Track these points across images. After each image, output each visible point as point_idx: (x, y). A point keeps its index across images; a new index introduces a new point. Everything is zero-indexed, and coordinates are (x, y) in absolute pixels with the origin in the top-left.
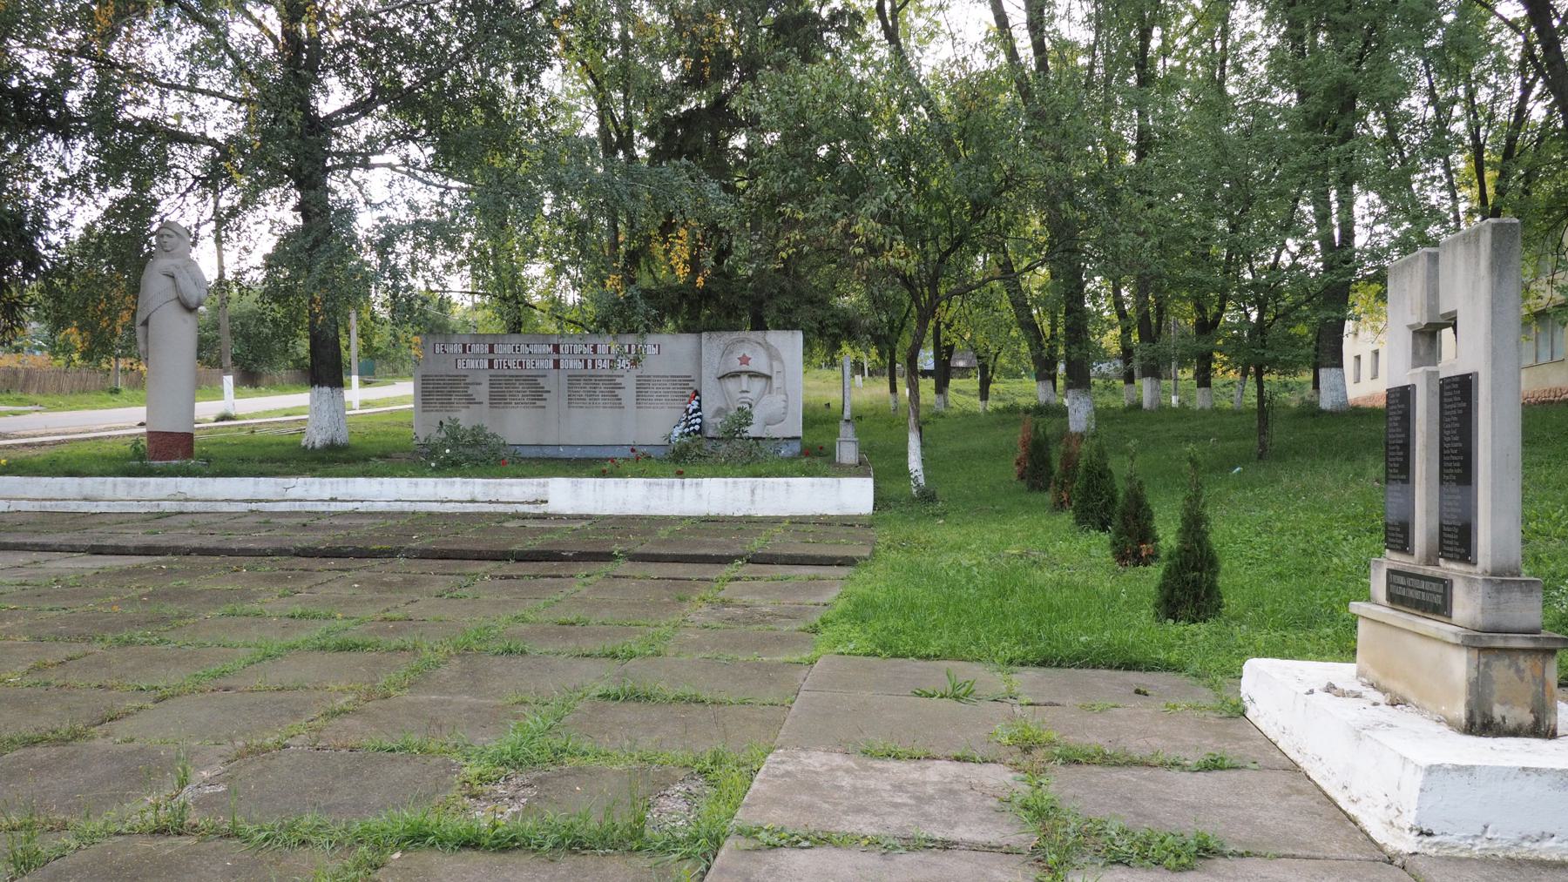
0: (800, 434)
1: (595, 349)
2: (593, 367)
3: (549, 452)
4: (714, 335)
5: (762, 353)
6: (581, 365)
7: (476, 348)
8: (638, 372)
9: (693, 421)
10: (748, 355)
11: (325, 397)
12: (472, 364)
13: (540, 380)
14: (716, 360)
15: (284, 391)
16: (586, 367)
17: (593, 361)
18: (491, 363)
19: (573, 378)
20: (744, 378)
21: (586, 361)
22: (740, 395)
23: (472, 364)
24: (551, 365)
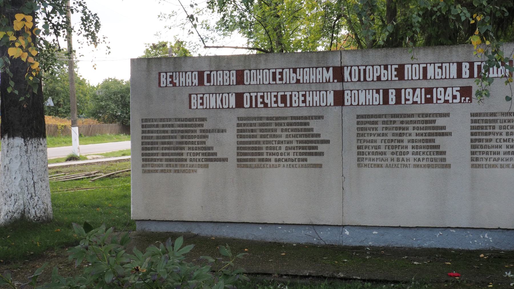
1: (400, 72)
2: (398, 101)
6: (378, 98)
7: (218, 78)
8: (476, 106)
11: (16, 152)
12: (212, 101)
13: (313, 124)
15: (110, 139)
16: (386, 101)
17: (398, 92)
18: (239, 98)
21: (386, 92)
23: (212, 101)
24: (331, 99)
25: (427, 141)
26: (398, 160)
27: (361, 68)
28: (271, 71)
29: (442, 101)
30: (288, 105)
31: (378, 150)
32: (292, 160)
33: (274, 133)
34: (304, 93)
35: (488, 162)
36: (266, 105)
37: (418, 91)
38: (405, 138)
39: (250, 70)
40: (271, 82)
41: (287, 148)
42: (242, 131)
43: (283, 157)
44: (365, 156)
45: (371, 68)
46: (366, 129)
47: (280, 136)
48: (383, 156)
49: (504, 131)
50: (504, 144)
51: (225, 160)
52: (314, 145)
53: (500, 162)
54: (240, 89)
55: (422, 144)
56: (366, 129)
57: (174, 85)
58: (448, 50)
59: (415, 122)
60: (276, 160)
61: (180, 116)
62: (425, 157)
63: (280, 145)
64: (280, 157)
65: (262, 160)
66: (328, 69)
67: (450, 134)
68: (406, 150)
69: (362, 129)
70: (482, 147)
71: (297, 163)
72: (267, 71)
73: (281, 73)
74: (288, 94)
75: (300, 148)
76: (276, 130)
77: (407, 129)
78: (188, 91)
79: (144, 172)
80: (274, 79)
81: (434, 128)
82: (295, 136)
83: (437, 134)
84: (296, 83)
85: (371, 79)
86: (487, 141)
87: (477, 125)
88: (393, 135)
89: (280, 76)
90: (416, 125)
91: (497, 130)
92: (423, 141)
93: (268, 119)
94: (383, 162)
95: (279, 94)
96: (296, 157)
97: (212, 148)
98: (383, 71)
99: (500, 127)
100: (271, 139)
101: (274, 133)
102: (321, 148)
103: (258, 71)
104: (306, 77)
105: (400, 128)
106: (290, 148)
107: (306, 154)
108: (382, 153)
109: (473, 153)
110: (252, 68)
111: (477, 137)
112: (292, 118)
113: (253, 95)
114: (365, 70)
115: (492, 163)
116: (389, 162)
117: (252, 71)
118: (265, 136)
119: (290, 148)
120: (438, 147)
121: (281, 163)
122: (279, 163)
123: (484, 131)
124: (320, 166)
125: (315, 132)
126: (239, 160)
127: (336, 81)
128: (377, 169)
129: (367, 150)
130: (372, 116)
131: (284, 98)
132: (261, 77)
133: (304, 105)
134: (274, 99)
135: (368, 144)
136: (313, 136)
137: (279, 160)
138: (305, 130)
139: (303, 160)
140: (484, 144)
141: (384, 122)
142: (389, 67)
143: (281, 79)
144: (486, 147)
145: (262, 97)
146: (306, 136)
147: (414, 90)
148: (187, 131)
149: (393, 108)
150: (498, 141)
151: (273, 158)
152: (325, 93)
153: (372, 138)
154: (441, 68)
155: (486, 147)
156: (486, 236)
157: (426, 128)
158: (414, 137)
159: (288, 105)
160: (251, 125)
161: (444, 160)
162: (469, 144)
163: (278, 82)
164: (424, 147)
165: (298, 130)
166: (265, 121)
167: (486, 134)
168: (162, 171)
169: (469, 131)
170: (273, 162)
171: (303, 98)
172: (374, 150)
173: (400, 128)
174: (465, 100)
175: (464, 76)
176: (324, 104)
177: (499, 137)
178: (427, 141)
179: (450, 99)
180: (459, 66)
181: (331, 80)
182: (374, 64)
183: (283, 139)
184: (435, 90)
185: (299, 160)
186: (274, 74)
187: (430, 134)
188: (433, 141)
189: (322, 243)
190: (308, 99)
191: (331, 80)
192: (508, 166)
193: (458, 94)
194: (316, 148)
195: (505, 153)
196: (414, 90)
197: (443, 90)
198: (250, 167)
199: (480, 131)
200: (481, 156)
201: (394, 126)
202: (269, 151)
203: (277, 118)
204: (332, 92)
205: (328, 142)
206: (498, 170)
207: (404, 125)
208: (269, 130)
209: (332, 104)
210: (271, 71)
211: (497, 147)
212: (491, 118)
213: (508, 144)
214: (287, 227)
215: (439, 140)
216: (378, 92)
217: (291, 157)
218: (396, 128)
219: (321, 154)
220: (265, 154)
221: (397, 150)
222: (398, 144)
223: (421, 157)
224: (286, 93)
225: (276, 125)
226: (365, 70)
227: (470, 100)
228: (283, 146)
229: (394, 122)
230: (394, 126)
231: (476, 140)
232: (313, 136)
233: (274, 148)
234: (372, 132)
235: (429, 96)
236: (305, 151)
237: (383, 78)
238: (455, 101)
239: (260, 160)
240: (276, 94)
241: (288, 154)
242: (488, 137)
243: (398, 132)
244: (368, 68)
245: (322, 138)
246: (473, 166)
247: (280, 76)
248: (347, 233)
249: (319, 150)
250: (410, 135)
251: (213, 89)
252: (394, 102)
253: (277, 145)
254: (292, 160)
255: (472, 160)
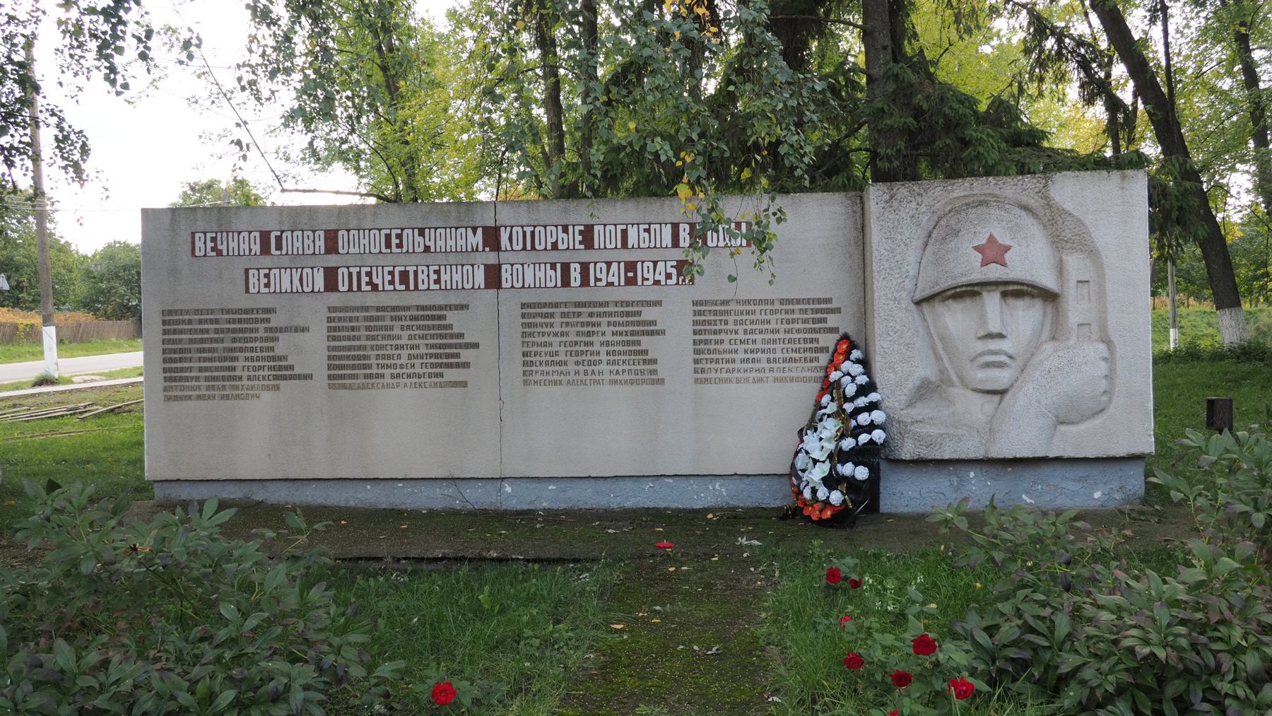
0: (1147, 445)
1: (587, 236)
2: (585, 282)
3: (477, 497)
4: (902, 190)
5: (1034, 230)
6: (555, 277)
7: (293, 242)
9: (864, 419)
10: (1003, 239)
12: (285, 281)
13: (452, 317)
14: (912, 256)
16: (566, 282)
17: (585, 267)
19: (534, 313)
20: (992, 300)
21: (566, 268)
22: (981, 346)
23: (285, 281)
25: (628, 343)
26: (586, 373)
27: (528, 230)
28: (383, 232)
29: (651, 282)
30: (412, 287)
31: (555, 359)
32: (419, 376)
33: (388, 333)
34: (437, 268)
35: (719, 375)
36: (375, 287)
37: (614, 266)
38: (596, 339)
39: (348, 231)
40: (384, 250)
41: (410, 357)
42: (335, 329)
43: (404, 370)
44: (534, 368)
45: (542, 229)
46: (535, 325)
47: (400, 337)
48: (563, 368)
49: (741, 328)
50: (741, 347)
51: (308, 377)
52: (454, 351)
53: (736, 375)
54: (331, 261)
55: (621, 348)
56: (535, 325)
57: (220, 253)
58: (658, 204)
59: (611, 314)
60: (392, 376)
61: (229, 306)
62: (626, 367)
63: (398, 352)
64: (399, 371)
65: (370, 376)
66: (474, 230)
67: (663, 332)
68: (597, 358)
69: (529, 325)
70: (709, 352)
71: (427, 380)
72: (377, 232)
73: (399, 236)
74: (411, 269)
75: (431, 356)
76: (392, 328)
77: (599, 324)
78: (243, 264)
79: (168, 399)
80: (388, 245)
81: (639, 323)
82: (424, 337)
83: (643, 333)
84: (424, 252)
85: (543, 247)
86: (717, 342)
87: (702, 318)
88: (578, 334)
89: (398, 241)
90: (612, 319)
91: (731, 326)
92: (624, 343)
93: (378, 309)
94: (562, 377)
95: (397, 270)
96: (425, 370)
97: (285, 358)
98: (561, 235)
99: (736, 323)
100: (384, 342)
101: (388, 333)
102: (466, 355)
103: (361, 232)
104: (440, 243)
105: (588, 324)
106: (416, 357)
107: (441, 365)
108: (560, 363)
109: (696, 361)
110: (351, 226)
111: (703, 337)
112: (419, 308)
113: (354, 271)
114: (533, 233)
115: (724, 375)
116: (572, 377)
117: (352, 232)
118: (374, 338)
119: (416, 357)
120: (645, 352)
121: (401, 380)
122: (398, 380)
123: (713, 327)
124: (464, 384)
125: (455, 330)
126: (330, 377)
127: (487, 249)
128: (553, 388)
129: (538, 358)
130: (545, 305)
131: (404, 276)
132: (366, 242)
133: (437, 287)
134: (388, 278)
135: (539, 349)
136: (452, 336)
137: (398, 376)
138: (440, 327)
139: (437, 375)
140: (712, 347)
141: (563, 315)
142: (571, 228)
143: (400, 246)
144: (715, 352)
145: (369, 274)
146: (442, 337)
147: (609, 264)
148: (241, 331)
149: (576, 292)
150: (733, 342)
151: (387, 372)
152: (470, 268)
153: (546, 339)
154: (647, 231)
155: (715, 352)
156: (717, 487)
157: (628, 324)
158: (609, 338)
159: (412, 287)
160: (351, 319)
161: (655, 372)
162: (691, 347)
163: (394, 249)
164: (625, 353)
165: (428, 328)
166: (374, 314)
167: (715, 332)
168: (199, 397)
169: (690, 328)
170: (388, 380)
171: (435, 277)
172: (548, 358)
173: (588, 324)
174: (684, 280)
175: (682, 244)
176: (470, 286)
177: (734, 336)
178: (628, 343)
179: (662, 278)
180: (675, 227)
181: (480, 248)
182: (547, 223)
183: (404, 342)
184: (639, 265)
185: (430, 376)
186: (388, 237)
187: (633, 333)
188: (639, 343)
189: (470, 507)
190: (444, 277)
191: (480, 248)
192: (747, 380)
193: (674, 271)
194: (457, 356)
195: (742, 361)
196: (609, 264)
197: (651, 265)
198: (351, 387)
199: (707, 327)
200: (709, 366)
201: (580, 320)
202: (381, 362)
203: (394, 309)
204: (482, 267)
205: (476, 346)
206: (734, 386)
207: (594, 319)
208: (381, 328)
209: (482, 286)
210: (383, 232)
211: (731, 352)
212: (723, 308)
213: (747, 346)
214: (413, 483)
215: (646, 342)
216: (553, 266)
217: (418, 370)
218: (582, 324)
219: (466, 365)
220: (374, 366)
221: (584, 357)
222: (585, 349)
223: (620, 368)
224: (408, 268)
225: (392, 319)
226: (533, 233)
227: (692, 280)
228: (405, 353)
229: (579, 314)
230: (580, 320)
231: (701, 341)
232: (452, 336)
233: (389, 357)
234: (544, 329)
235: (630, 274)
236: (439, 361)
237: (560, 246)
238: (669, 282)
239: (366, 376)
240: (391, 269)
241: (413, 366)
242: (718, 337)
243: (586, 329)
244: (537, 230)
245: (467, 340)
246: (696, 380)
247: (398, 241)
248: (509, 489)
249: (462, 360)
250: (604, 334)
251: (285, 261)
252: (578, 283)
253: (394, 352)
254: (419, 376)
255: (696, 372)
